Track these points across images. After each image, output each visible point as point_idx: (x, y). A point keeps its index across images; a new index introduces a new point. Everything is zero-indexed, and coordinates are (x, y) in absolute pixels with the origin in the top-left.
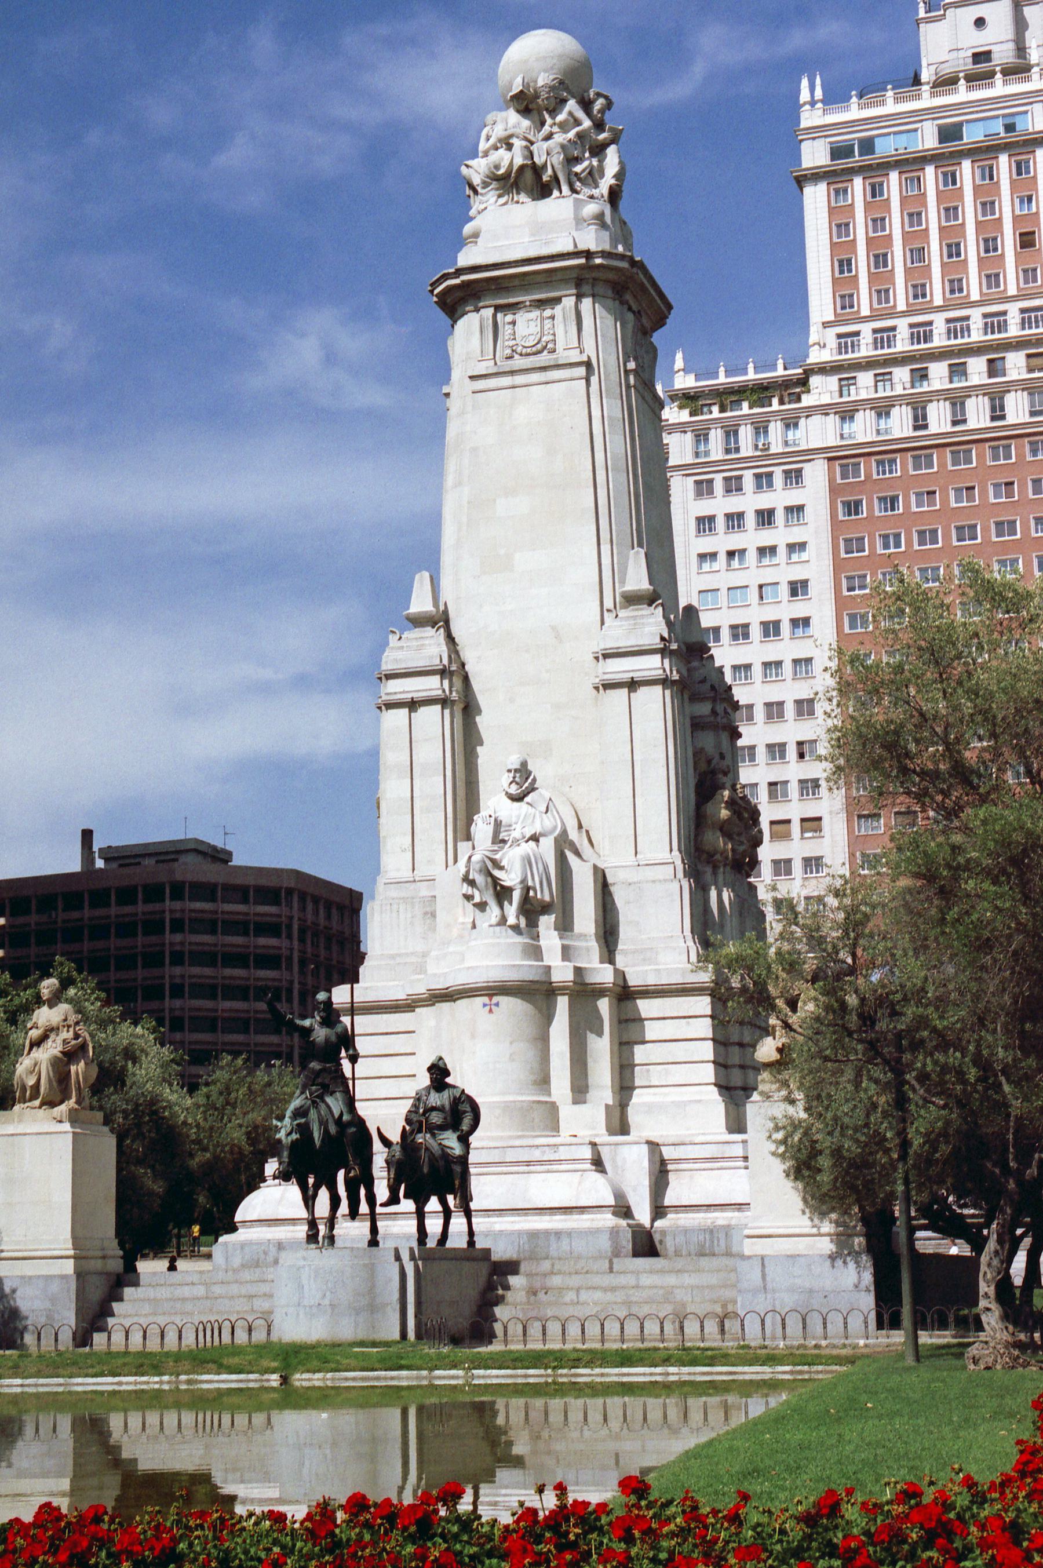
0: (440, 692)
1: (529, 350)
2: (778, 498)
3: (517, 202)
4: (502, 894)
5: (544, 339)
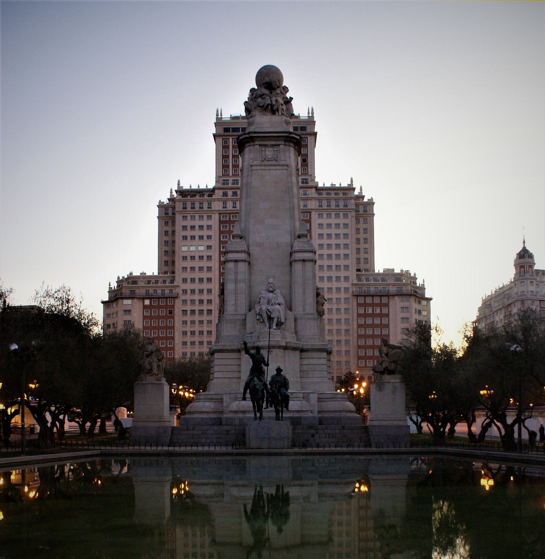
0: (245, 258)
1: (269, 159)
2: (205, 222)
3: (265, 115)
4: (270, 319)
5: (275, 157)
